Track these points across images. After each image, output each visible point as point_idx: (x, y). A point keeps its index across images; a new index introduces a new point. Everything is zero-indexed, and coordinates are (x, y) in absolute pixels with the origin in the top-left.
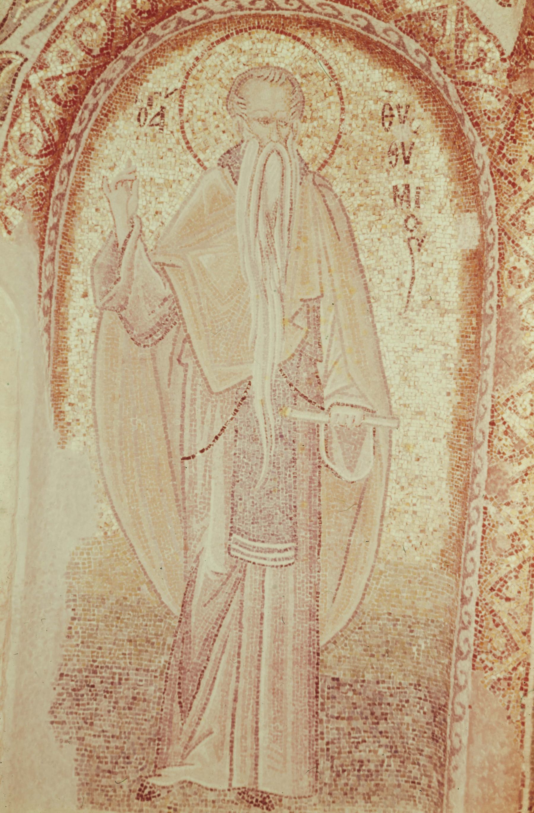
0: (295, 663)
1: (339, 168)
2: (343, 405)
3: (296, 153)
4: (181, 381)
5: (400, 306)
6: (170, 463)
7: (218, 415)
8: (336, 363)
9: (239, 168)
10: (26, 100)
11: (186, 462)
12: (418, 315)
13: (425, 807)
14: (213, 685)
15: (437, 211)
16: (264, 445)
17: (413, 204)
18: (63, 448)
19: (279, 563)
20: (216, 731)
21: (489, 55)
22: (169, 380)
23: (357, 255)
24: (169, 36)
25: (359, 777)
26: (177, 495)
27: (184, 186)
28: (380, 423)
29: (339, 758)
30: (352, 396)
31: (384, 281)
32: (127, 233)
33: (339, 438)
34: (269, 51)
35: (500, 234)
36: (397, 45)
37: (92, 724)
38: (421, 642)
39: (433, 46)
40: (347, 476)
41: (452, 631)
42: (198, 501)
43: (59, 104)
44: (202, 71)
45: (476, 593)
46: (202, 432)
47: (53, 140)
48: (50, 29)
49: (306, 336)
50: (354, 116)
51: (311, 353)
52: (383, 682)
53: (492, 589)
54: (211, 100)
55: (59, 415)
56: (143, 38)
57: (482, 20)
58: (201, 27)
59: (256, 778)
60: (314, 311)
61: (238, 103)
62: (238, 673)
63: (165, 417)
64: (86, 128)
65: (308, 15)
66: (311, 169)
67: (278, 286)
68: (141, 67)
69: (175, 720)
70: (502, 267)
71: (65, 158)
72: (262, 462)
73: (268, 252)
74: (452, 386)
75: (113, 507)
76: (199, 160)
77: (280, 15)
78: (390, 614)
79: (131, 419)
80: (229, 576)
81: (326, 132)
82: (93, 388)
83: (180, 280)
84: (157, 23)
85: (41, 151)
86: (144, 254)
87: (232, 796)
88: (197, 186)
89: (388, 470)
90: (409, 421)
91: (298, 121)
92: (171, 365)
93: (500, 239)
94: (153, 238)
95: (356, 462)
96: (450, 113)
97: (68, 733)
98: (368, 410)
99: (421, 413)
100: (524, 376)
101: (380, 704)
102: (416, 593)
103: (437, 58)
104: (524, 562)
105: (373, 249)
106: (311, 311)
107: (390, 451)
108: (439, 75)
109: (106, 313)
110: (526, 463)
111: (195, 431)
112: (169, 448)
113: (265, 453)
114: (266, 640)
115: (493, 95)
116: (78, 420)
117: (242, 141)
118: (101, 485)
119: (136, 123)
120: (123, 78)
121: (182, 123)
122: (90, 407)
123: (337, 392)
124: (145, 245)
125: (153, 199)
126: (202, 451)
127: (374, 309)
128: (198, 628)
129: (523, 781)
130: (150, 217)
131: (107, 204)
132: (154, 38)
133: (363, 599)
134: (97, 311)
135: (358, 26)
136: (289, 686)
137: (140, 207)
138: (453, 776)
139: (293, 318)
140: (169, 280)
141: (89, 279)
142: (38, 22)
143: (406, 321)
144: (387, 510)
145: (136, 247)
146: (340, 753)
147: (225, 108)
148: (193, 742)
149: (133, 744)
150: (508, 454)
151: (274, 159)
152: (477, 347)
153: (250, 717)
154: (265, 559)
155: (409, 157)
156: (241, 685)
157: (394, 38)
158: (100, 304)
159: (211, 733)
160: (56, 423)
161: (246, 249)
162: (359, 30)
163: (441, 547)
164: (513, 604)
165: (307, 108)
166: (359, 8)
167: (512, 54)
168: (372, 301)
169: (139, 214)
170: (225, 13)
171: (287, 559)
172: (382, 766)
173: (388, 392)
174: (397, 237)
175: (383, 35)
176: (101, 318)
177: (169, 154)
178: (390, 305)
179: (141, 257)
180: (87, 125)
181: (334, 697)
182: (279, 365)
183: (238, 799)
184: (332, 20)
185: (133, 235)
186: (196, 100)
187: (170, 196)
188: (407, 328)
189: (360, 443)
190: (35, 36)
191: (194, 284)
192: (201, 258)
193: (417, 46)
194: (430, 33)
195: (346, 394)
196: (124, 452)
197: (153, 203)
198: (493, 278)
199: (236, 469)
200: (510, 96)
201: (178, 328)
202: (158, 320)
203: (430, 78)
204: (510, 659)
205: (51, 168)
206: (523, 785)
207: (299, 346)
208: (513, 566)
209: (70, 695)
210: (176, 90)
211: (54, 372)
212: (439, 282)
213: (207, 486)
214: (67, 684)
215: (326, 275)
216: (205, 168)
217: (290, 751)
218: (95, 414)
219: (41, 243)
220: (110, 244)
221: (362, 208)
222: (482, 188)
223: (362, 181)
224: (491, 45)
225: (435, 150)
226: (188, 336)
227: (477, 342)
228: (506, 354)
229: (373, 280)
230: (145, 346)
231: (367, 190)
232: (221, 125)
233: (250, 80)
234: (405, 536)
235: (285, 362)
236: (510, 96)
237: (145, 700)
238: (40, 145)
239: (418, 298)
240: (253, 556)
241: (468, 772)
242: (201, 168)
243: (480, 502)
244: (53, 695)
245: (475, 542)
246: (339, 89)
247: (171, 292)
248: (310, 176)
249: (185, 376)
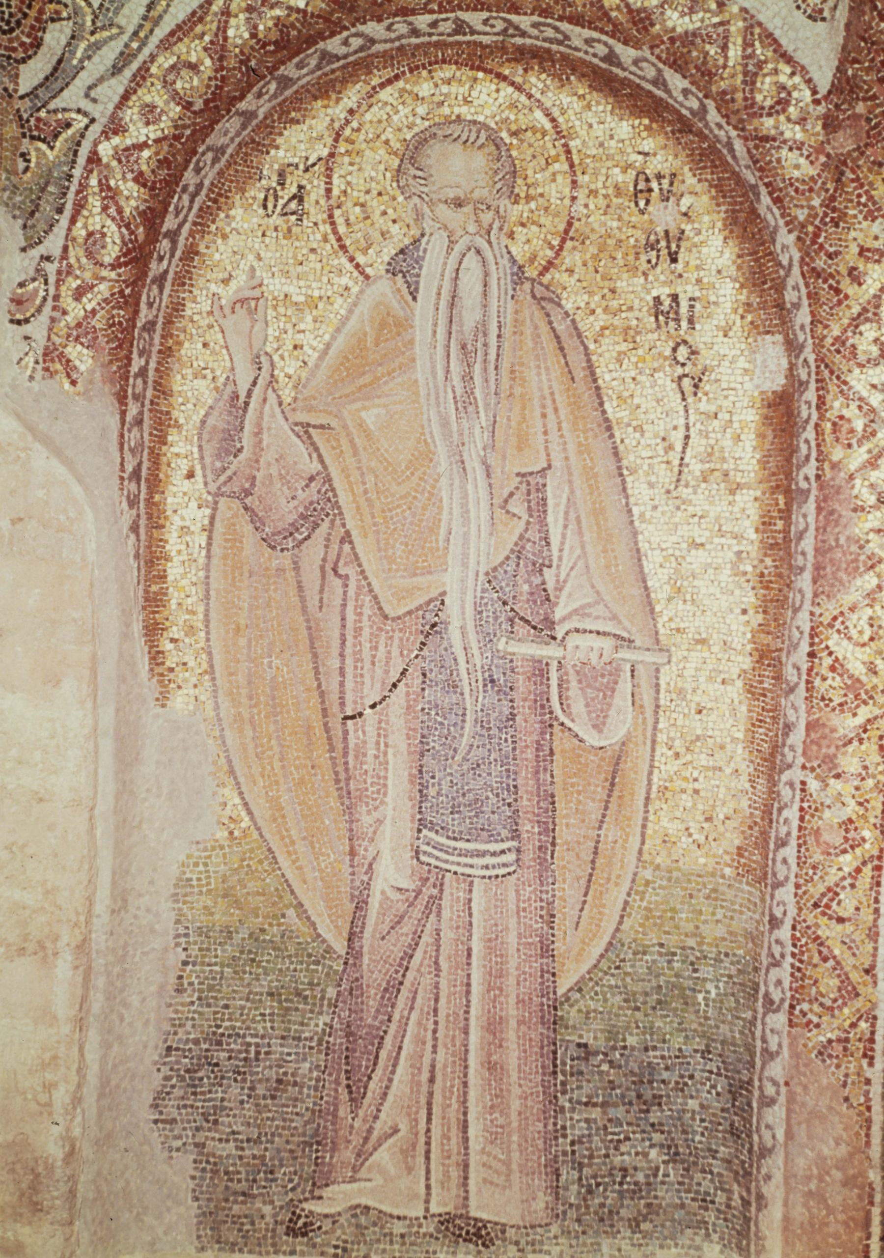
0: (520, 1022)
1: (570, 271)
2: (585, 631)
4: (338, 602)
5: (667, 480)
6: (326, 725)
7: (395, 652)
8: (572, 568)
9: (418, 276)
10: (94, 181)
11: (350, 722)
12: (695, 493)
13: (722, 1239)
14: (397, 1058)
15: (721, 334)
16: (467, 696)
17: (684, 324)
18: (163, 706)
19: (493, 872)
20: (403, 1127)
21: (795, 94)
22: (321, 600)
23: (601, 404)
24: (308, 78)
25: (621, 1193)
26: (336, 773)
27: (336, 306)
28: (640, 658)
29: (590, 1165)
30: (597, 618)
31: (643, 441)
32: (252, 379)
33: (580, 682)
34: (460, 97)
35: (818, 367)
36: (655, 82)
37: (216, 1122)
38: (710, 986)
39: (710, 82)
40: (592, 739)
41: (756, 970)
42: (369, 781)
43: (144, 185)
44: (358, 130)
45: (792, 911)
46: (372, 678)
47: (136, 240)
48: (128, 73)
49: (527, 530)
50: (591, 191)
51: (534, 554)
52: (655, 1048)
53: (816, 905)
54: (373, 174)
55: (156, 657)
56: (269, 83)
57: (783, 42)
58: (355, 63)
59: (466, 1198)
60: (538, 490)
61: (415, 177)
62: (435, 1039)
63: (315, 656)
64: (185, 221)
65: (519, 41)
68: (267, 126)
69: (341, 1113)
70: (822, 417)
71: (155, 268)
72: (463, 721)
73: (466, 402)
74: (750, 599)
75: (241, 793)
76: (357, 266)
77: (475, 43)
78: (661, 945)
79: (266, 661)
80: (419, 893)
82: (206, 615)
83: (333, 448)
84: (290, 59)
85: (118, 258)
86: (277, 410)
87: (429, 1227)
88: (355, 305)
89: (655, 728)
90: (686, 653)
91: (507, 202)
92: (323, 577)
93: (817, 373)
94: (290, 385)
95: (605, 717)
96: (737, 184)
97: (180, 1137)
98: (623, 639)
99: (703, 642)
100: (859, 582)
101: (650, 1082)
102: (700, 912)
103: (715, 100)
104: (864, 863)
105: (626, 394)
106: (533, 491)
107: (657, 699)
108: (720, 127)
109: (222, 501)
110: (865, 713)
111: (362, 676)
112: (323, 702)
113: (468, 706)
114: (475, 989)
115: (802, 155)
116: (185, 664)
117: (423, 235)
118: (223, 760)
119: (261, 211)
120: (240, 144)
121: (331, 209)
122: (202, 644)
123: (575, 611)
124: (279, 397)
125: (289, 326)
126: (373, 706)
127: (629, 485)
128: (374, 973)
129: (871, 1196)
130: (286, 354)
131: (220, 335)
132: (285, 82)
133: (621, 923)
134: (210, 498)
135: (595, 55)
136: (512, 1057)
137: (270, 339)
138: (765, 1190)
139: (506, 501)
140: (317, 449)
141: (195, 450)
142: (109, 63)
143: (678, 502)
144: (654, 788)
145: (265, 400)
146: (591, 1157)
147: (395, 185)
148: (369, 1146)
149: (278, 1151)
150: (837, 700)
151: (471, 261)
152: (787, 540)
153: (455, 1106)
154: (472, 866)
155: (676, 253)
156: (441, 1056)
157: (651, 73)
158: (213, 487)
159: (396, 1131)
160: (152, 670)
161: (433, 398)
162: (596, 61)
163: (737, 842)
164: (849, 927)
165: (520, 181)
166: (596, 29)
167: (830, 92)
168: (625, 472)
169: (268, 349)
170: (392, 41)
171: (505, 865)
172: (655, 1176)
173: (652, 611)
174: (661, 374)
175: (633, 68)
176: (215, 509)
177: (312, 257)
178: (653, 479)
179: (273, 416)
180: (186, 216)
181: (581, 1073)
182: (487, 574)
183: (439, 1231)
184: (554, 47)
185: (260, 381)
186: (350, 173)
187: (315, 321)
188: (679, 513)
189: (611, 689)
190: (106, 84)
191: (355, 453)
192: (363, 414)
193: (686, 84)
194: (705, 63)
195: (589, 615)
196: (255, 711)
197: (290, 332)
198: (810, 434)
199: (425, 732)
200: (828, 156)
201: (332, 522)
202: (301, 510)
203: (706, 132)
204: (846, 1011)
205: (134, 284)
206: (872, 1203)
207: (516, 544)
208: (847, 870)
209: (183, 1079)
210: (320, 159)
211: (146, 592)
212: (727, 443)
213: (381, 759)
214: (178, 1062)
215: (553, 436)
216: (367, 277)
217: (515, 1155)
218: (210, 654)
219: (122, 398)
220: (225, 397)
221: (607, 332)
222: (790, 296)
223: (606, 291)
224: (797, 79)
225: (717, 240)
226: (348, 533)
227: (786, 531)
228: (830, 549)
229: (627, 441)
230: (282, 550)
231: (614, 304)
232: (390, 211)
233: (432, 142)
234: (682, 827)
235: (495, 569)
236: (828, 156)
237: (295, 1084)
238: (117, 248)
239: (695, 467)
240: (453, 863)
241: (786, 1183)
242: (361, 278)
243: (796, 774)
244: (157, 1080)
245: (788, 834)
246: (568, 152)
247: (320, 467)
248: (527, 286)
249: (345, 593)
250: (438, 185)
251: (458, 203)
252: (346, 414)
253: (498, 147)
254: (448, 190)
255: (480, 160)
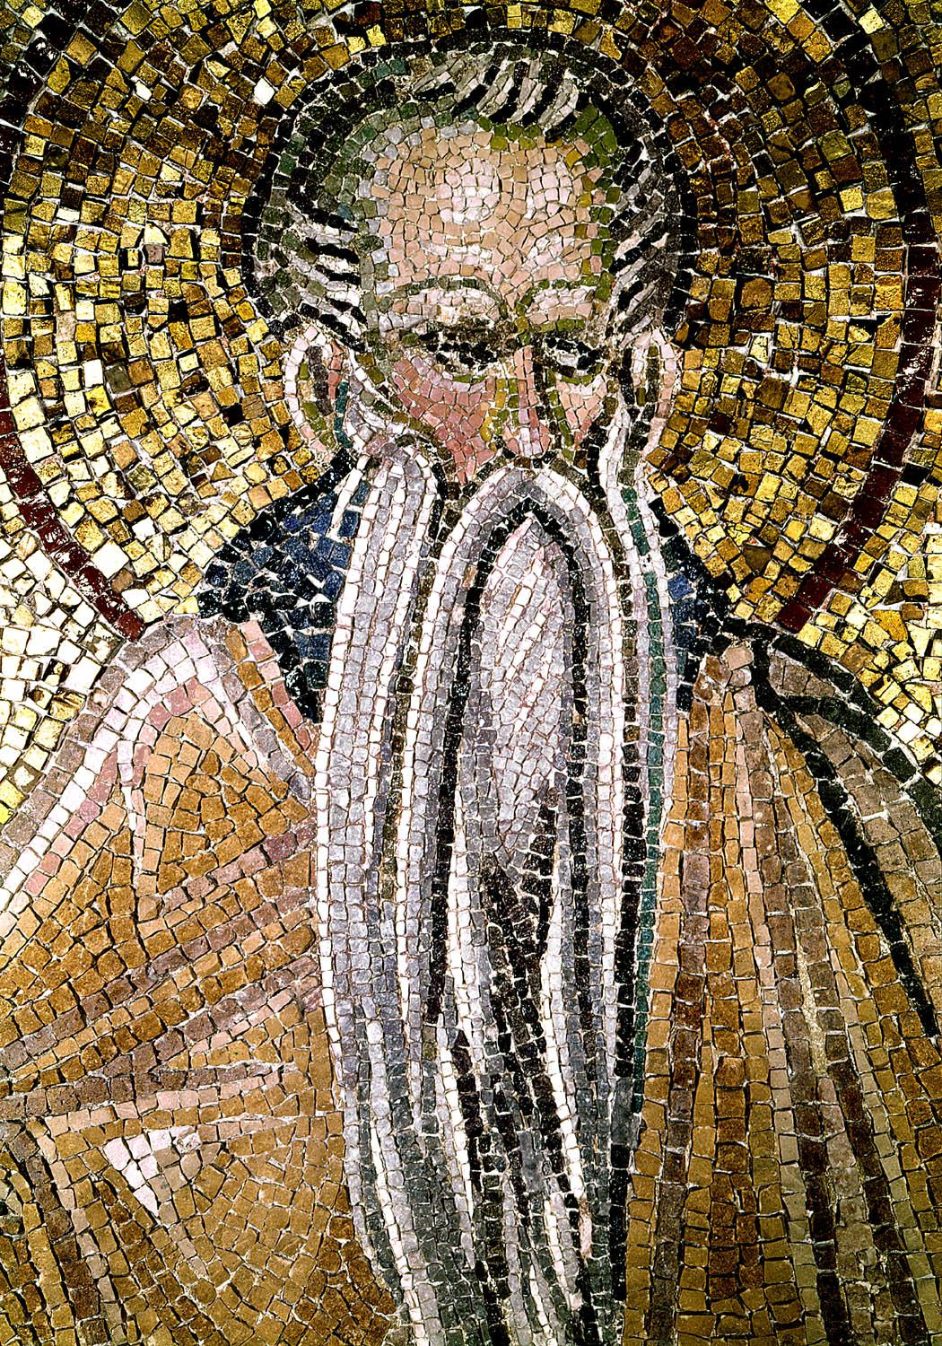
3: (650, 522)
9: (326, 616)
44: (99, 70)
54: (154, 236)
61: (312, 248)
66: (743, 612)
67: (575, 1302)
81: (827, 396)
91: (657, 336)
117: (342, 465)
147: (233, 277)
151: (523, 569)
186: (70, 234)
216: (132, 624)
232: (219, 377)
246: (897, 150)
248: (739, 656)
250: (400, 275)
251: (476, 343)
252: (47, 1148)
253: (626, 134)
254: (434, 294)
255: (555, 182)
